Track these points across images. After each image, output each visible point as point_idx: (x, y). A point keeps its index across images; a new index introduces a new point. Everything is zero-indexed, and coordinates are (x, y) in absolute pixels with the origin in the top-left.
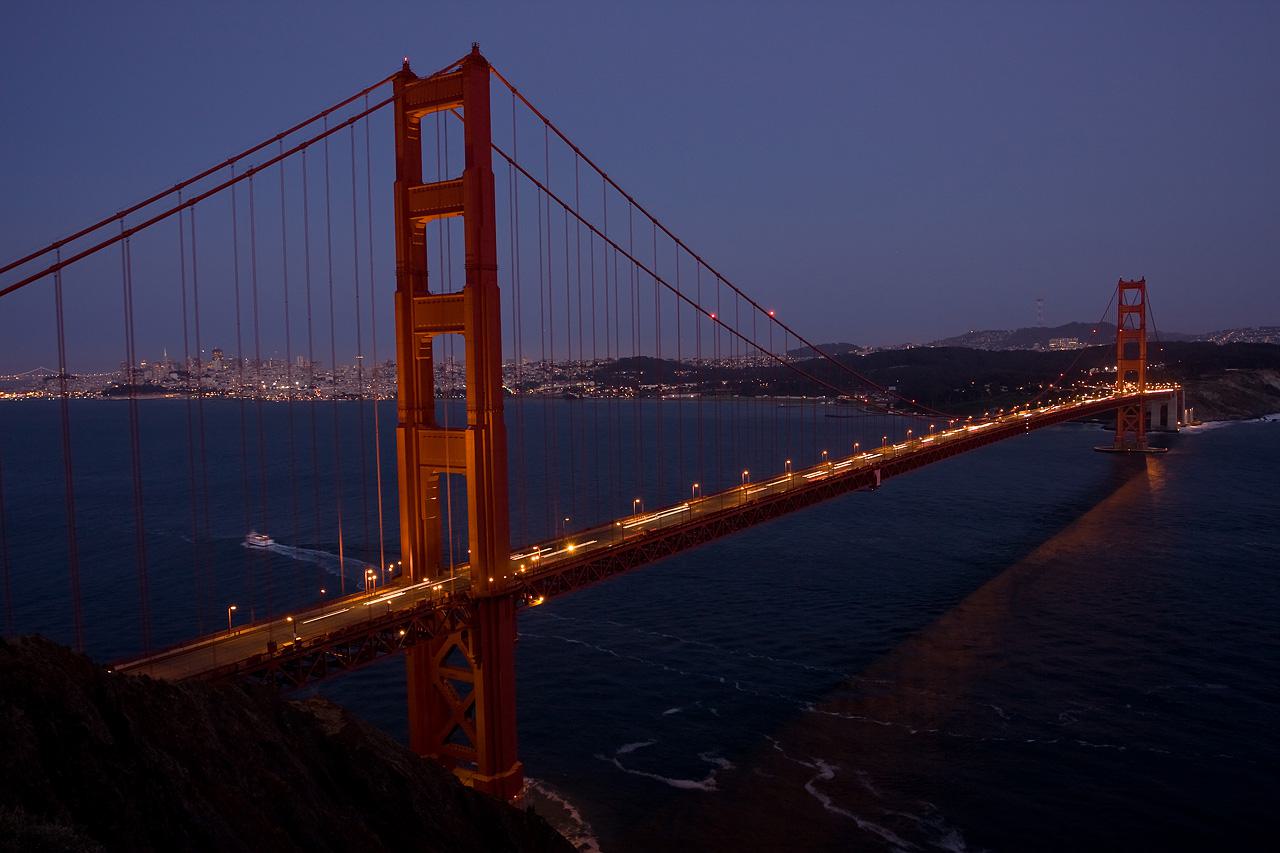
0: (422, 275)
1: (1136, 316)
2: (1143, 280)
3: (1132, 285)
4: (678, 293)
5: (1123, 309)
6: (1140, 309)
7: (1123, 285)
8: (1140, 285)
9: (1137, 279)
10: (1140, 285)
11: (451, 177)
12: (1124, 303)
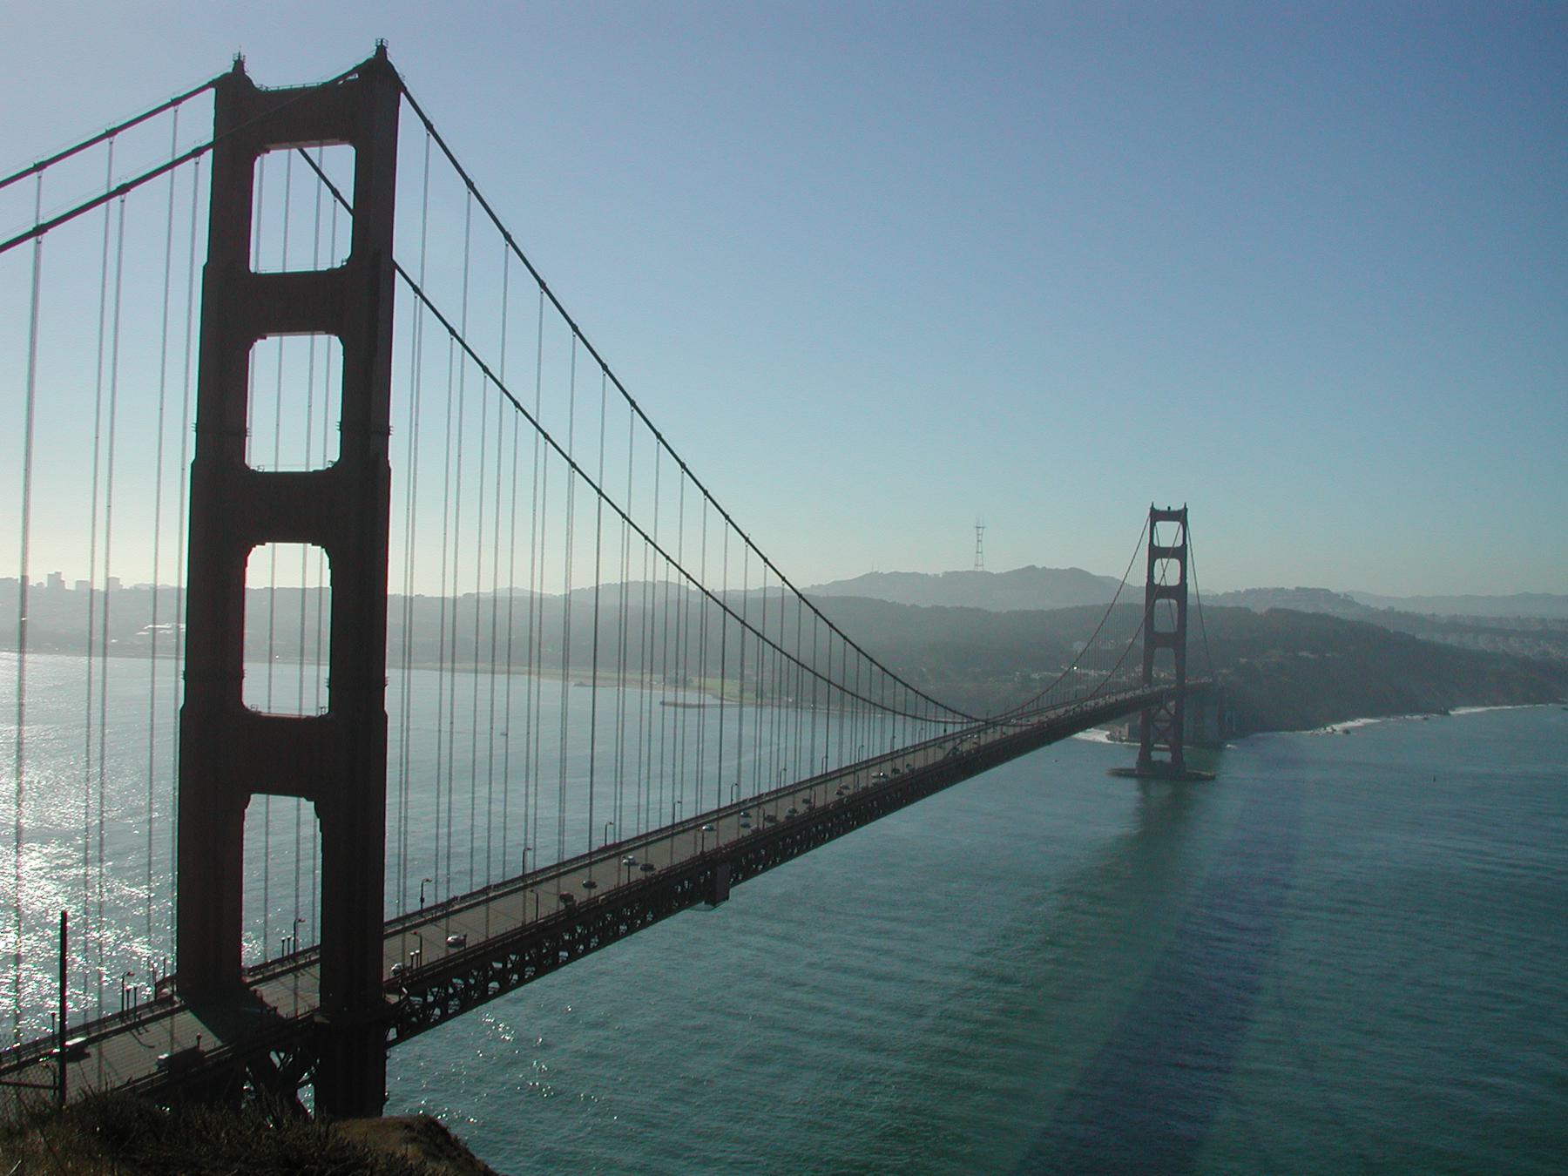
0: (240, 433)
1: (1175, 563)
2: (1185, 509)
3: (1169, 515)
4: (599, 492)
5: (1156, 553)
6: (1180, 553)
7: (1156, 516)
8: (1180, 516)
9: (1172, 509)
10: (1180, 516)
11: (323, 266)
12: (1156, 544)
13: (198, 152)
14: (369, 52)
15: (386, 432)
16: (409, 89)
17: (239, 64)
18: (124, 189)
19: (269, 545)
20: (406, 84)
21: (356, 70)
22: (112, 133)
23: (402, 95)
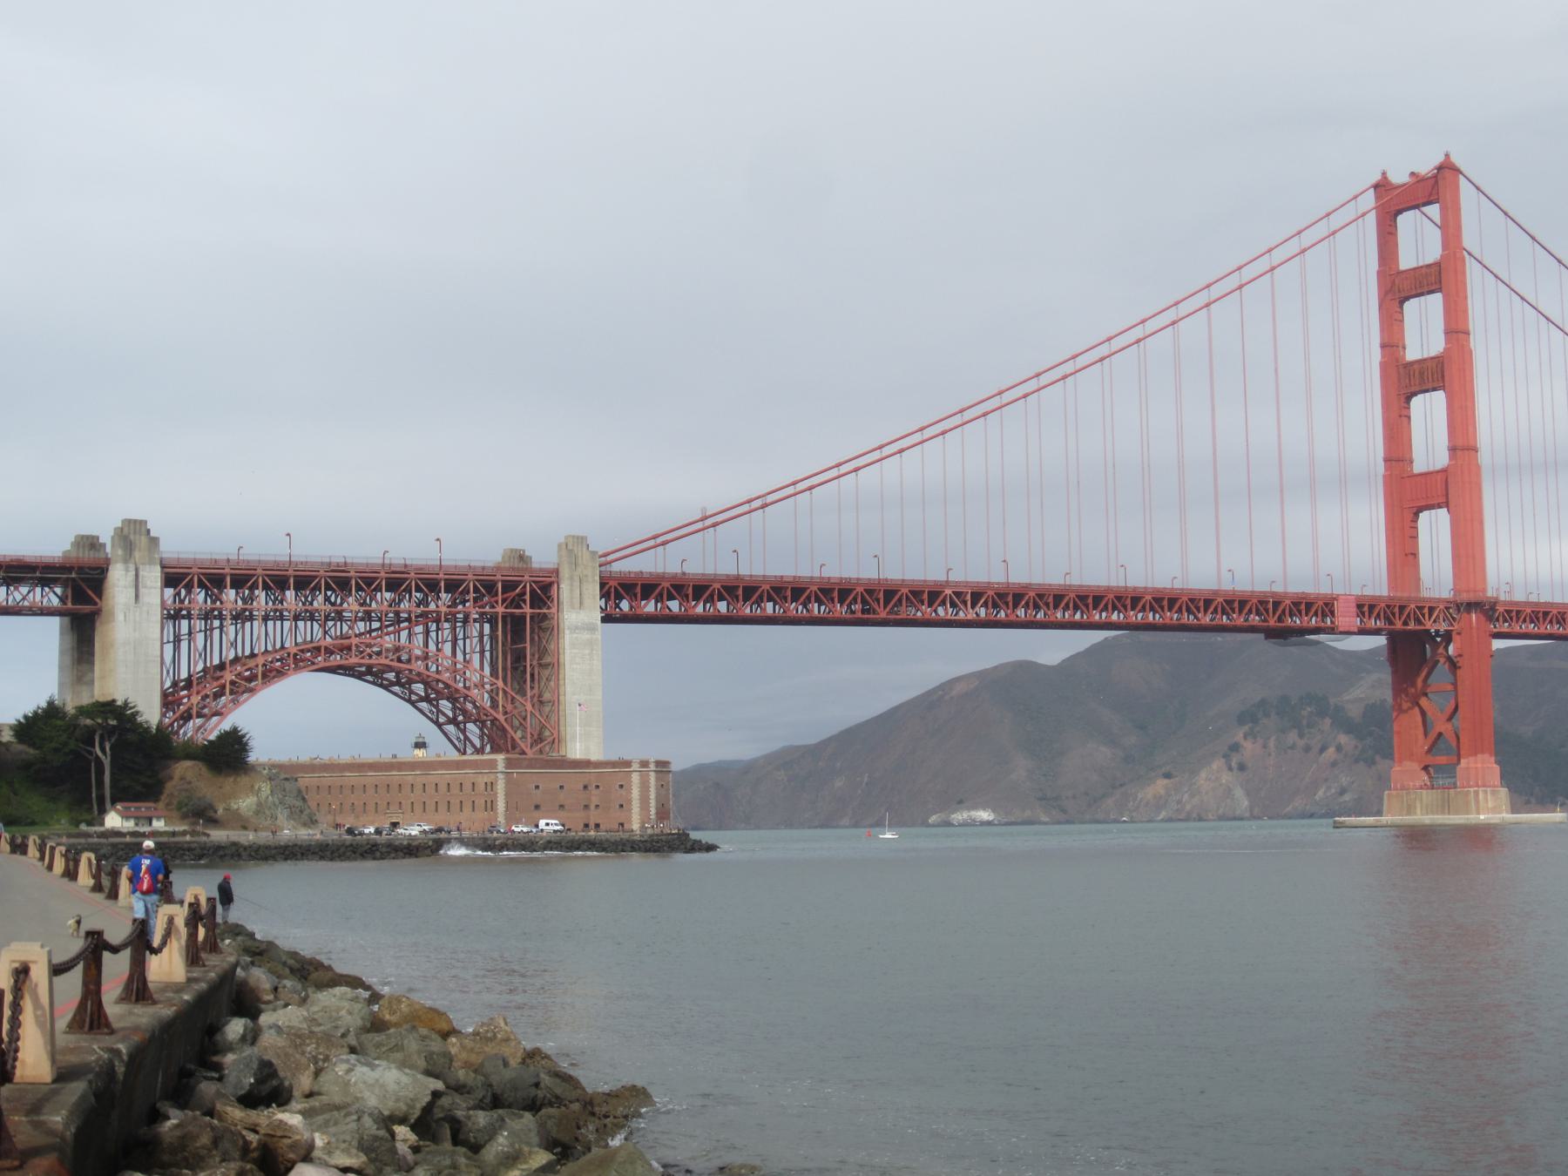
13: (1364, 215)
14: (1441, 158)
15: (1469, 334)
16: (1464, 172)
17: (1384, 174)
18: (1334, 233)
19: (1420, 397)
20: (1462, 169)
21: (1435, 168)
22: (1328, 215)
23: (1461, 176)
